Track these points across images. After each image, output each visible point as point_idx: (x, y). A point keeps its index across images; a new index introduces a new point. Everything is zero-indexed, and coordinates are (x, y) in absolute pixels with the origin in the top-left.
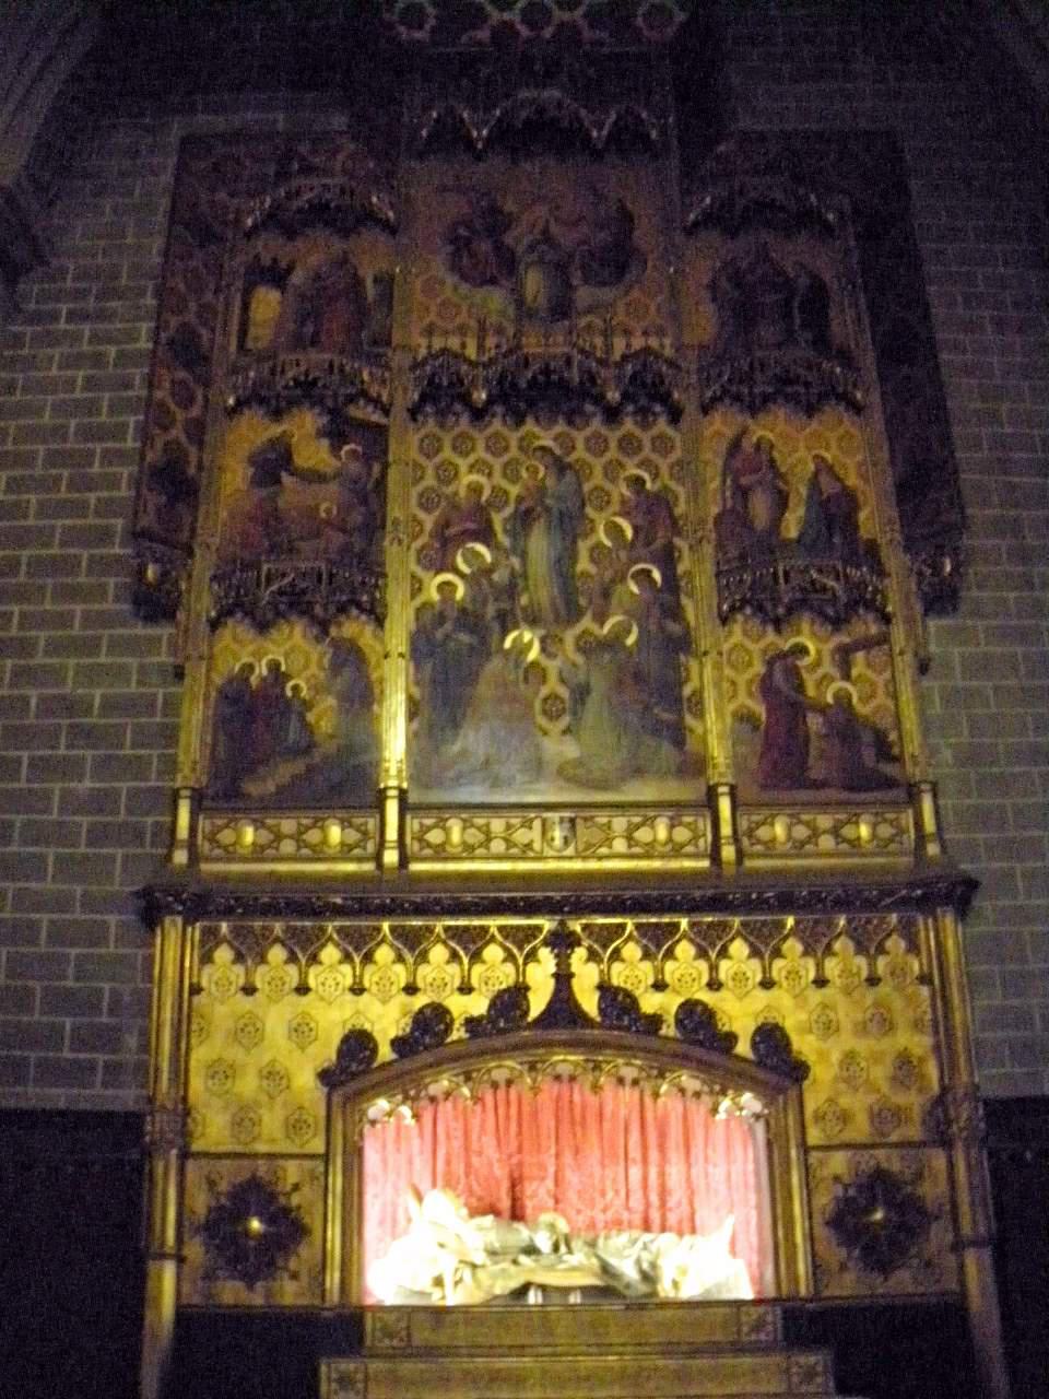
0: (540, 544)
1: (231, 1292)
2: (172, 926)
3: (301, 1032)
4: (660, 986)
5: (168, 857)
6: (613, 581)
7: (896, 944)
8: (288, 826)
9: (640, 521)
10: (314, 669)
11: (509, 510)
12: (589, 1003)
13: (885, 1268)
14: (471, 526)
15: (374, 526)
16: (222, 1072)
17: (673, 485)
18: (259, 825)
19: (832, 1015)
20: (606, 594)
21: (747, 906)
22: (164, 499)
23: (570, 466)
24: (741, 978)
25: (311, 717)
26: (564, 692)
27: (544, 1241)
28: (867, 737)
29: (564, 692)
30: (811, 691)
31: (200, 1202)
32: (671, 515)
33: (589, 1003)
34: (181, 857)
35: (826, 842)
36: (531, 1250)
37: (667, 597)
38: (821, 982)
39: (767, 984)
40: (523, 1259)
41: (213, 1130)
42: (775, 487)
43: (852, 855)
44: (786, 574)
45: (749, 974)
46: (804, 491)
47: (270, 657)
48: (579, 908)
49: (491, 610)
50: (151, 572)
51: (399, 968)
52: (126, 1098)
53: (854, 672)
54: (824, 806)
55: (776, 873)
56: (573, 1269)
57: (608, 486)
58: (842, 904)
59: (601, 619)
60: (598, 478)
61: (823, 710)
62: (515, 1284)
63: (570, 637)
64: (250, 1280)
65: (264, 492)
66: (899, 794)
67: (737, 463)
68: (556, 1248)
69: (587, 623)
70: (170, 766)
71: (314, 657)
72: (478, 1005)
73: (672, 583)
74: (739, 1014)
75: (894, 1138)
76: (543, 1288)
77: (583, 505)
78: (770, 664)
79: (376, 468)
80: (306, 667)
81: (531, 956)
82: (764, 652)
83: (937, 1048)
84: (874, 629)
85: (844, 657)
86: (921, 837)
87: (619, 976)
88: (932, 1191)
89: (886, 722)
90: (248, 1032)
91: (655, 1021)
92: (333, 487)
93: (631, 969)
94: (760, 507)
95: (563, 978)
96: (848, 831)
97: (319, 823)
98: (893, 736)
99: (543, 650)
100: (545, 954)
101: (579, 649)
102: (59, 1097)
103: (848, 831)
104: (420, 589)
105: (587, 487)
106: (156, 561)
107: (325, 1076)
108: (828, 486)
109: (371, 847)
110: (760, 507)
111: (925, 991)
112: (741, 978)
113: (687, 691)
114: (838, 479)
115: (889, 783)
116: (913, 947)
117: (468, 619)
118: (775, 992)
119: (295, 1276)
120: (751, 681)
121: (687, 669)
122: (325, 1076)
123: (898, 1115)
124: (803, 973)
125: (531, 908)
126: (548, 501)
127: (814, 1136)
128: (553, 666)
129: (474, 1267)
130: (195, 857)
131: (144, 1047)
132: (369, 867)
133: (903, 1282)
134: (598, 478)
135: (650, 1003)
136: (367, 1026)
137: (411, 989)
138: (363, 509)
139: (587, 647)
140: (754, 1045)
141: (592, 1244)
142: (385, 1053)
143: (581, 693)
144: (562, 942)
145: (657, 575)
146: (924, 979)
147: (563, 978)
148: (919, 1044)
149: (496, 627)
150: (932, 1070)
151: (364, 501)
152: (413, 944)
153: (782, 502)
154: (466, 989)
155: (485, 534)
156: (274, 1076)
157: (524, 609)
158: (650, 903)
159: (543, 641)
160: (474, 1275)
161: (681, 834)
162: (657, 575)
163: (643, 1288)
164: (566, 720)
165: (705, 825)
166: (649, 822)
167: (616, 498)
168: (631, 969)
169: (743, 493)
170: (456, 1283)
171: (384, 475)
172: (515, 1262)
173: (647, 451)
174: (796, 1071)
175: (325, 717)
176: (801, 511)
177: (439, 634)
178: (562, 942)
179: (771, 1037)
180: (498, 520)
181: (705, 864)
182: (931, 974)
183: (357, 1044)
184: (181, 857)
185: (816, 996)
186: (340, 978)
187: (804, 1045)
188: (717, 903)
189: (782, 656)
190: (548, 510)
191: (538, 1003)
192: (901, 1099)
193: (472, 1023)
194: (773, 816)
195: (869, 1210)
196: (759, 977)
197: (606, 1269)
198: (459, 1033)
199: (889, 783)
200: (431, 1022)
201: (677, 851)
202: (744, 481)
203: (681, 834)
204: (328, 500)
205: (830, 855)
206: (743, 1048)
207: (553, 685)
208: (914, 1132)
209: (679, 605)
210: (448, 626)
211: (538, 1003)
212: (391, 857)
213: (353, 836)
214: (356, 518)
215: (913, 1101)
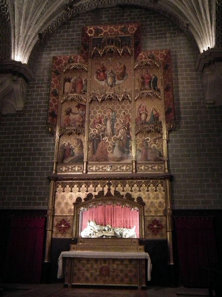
0: (109, 124)
1: (60, 236)
2: (52, 182)
3: (71, 197)
4: (123, 191)
5: (52, 172)
6: (120, 129)
7: (160, 185)
8: (70, 167)
9: (124, 120)
10: (74, 144)
11: (104, 118)
12: (113, 193)
13: (156, 234)
14: (98, 121)
15: (83, 122)
16: (60, 204)
17: (130, 113)
18: (66, 167)
19: (149, 196)
20: (118, 131)
21: (137, 179)
22: (51, 118)
23: (114, 111)
24: (135, 190)
25: (74, 151)
26: (111, 147)
27: (106, 229)
28: (158, 153)
29: (111, 147)
30: (149, 146)
31: (55, 223)
32: (129, 118)
33: (113, 193)
34: (54, 172)
35: (150, 169)
36: (105, 230)
37: (128, 132)
38: (148, 191)
39: (140, 191)
40: (103, 231)
41: (58, 213)
42: (146, 114)
43: (154, 171)
44: (145, 128)
45: (137, 189)
46: (150, 114)
47: (68, 142)
48: (111, 179)
49: (101, 134)
50: (50, 129)
51: (85, 188)
52: (45, 208)
53: (156, 143)
54: (150, 164)
55: (142, 174)
56: (111, 233)
57: (119, 114)
58: (151, 179)
59: (117, 135)
60: (118, 113)
61: (151, 149)
62: (101, 235)
63: (112, 138)
64: (62, 234)
65: (67, 116)
66: (162, 162)
67: (140, 110)
68: (108, 230)
69: (115, 136)
70: (53, 159)
71: (75, 142)
72: (97, 194)
73: (129, 129)
74: (135, 195)
75: (158, 215)
76: (106, 236)
77: (115, 118)
78: (143, 142)
79: (84, 112)
80: (73, 143)
81: (104, 186)
82: (142, 140)
83: (165, 202)
84: (160, 136)
85: (155, 141)
86: (165, 169)
87: (117, 189)
88: (163, 223)
89: (161, 151)
90: (63, 197)
91: (123, 196)
92: (78, 115)
93: (119, 188)
94: (143, 116)
95: (109, 190)
96: (154, 168)
97: (75, 167)
98: (162, 153)
99: (108, 140)
100: (106, 186)
101: (114, 140)
102: (36, 208)
103: (154, 168)
104: (90, 131)
105: (116, 114)
106: (50, 128)
107: (74, 204)
108: (154, 113)
109: (82, 170)
110: (143, 116)
111: (164, 193)
112: (135, 190)
113: (130, 146)
114: (156, 111)
115: (161, 160)
116: (162, 186)
117: (98, 136)
118: (141, 192)
119: (68, 234)
120: (139, 145)
121: (130, 143)
122: (74, 204)
123: (159, 211)
124: (145, 189)
125: (105, 179)
126: (110, 117)
127: (146, 214)
128: (110, 142)
129: (96, 232)
130: (56, 172)
131: (48, 200)
132: (82, 173)
133: (158, 237)
134: (118, 113)
135: (122, 193)
136: (80, 197)
137: (87, 191)
138: (82, 119)
139: (115, 139)
140: (137, 200)
141: (114, 230)
142: (83, 201)
143: (114, 146)
144: (109, 184)
145: (126, 128)
146: (164, 191)
147: (109, 190)
148: (163, 201)
149: (102, 137)
150: (164, 204)
151: (82, 118)
152: (88, 186)
153: (147, 115)
154: (95, 191)
155: (100, 122)
156: (67, 204)
157: (106, 134)
158: (122, 179)
159: (108, 139)
160: (95, 234)
161: (128, 168)
162: (126, 128)
163: (121, 236)
164: (111, 151)
165: (131, 166)
166: (123, 166)
167: (121, 116)
168: (119, 188)
169: (141, 114)
170: (93, 235)
171: (85, 112)
172: (102, 232)
173: (126, 108)
174: (143, 204)
175: (76, 151)
176: (150, 117)
177: (93, 138)
178: (109, 184)
179: (140, 199)
180: (102, 120)
181: (131, 172)
182: (165, 190)
183: (79, 199)
184: (54, 172)
185: (147, 193)
186: (77, 190)
187: (145, 200)
188: (132, 179)
189: (145, 140)
190: (110, 118)
191: (105, 193)
192: (160, 209)
193: (95, 196)
194: (142, 165)
195: (153, 226)
196: (138, 190)
197: (115, 233)
198: (94, 198)
199: (161, 160)
200: (89, 196)
201: (127, 170)
202: (141, 112)
203: (128, 168)
204: (77, 117)
205: (150, 171)
206: (135, 201)
207: (110, 145)
208: (161, 214)
209: (129, 133)
210: (94, 137)
211: (105, 193)
212: (85, 172)
213: (80, 168)
214: (81, 120)
215: (162, 209)
